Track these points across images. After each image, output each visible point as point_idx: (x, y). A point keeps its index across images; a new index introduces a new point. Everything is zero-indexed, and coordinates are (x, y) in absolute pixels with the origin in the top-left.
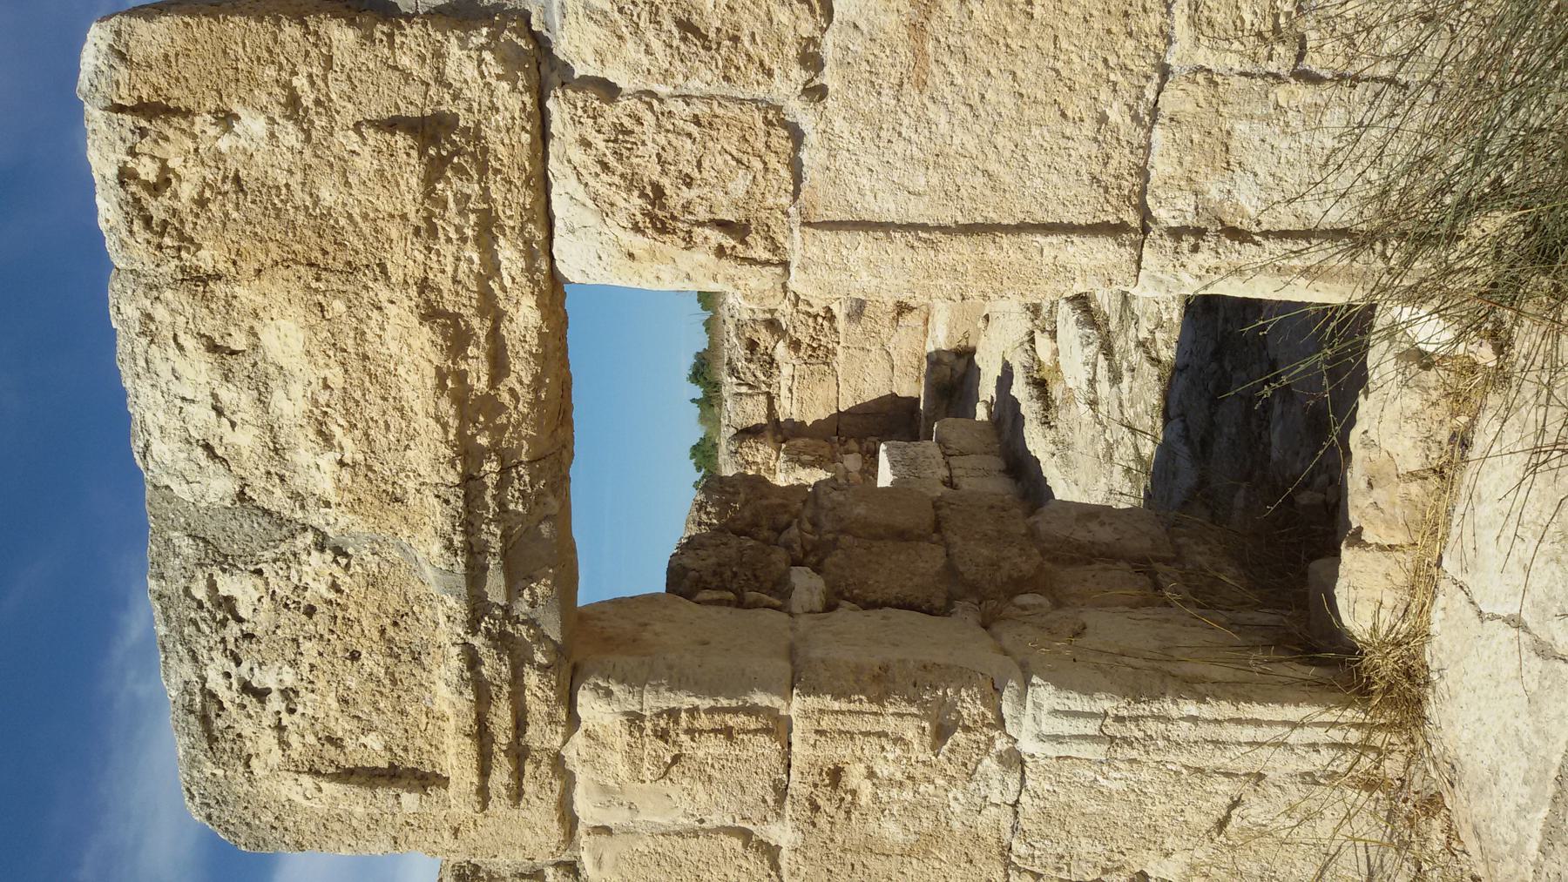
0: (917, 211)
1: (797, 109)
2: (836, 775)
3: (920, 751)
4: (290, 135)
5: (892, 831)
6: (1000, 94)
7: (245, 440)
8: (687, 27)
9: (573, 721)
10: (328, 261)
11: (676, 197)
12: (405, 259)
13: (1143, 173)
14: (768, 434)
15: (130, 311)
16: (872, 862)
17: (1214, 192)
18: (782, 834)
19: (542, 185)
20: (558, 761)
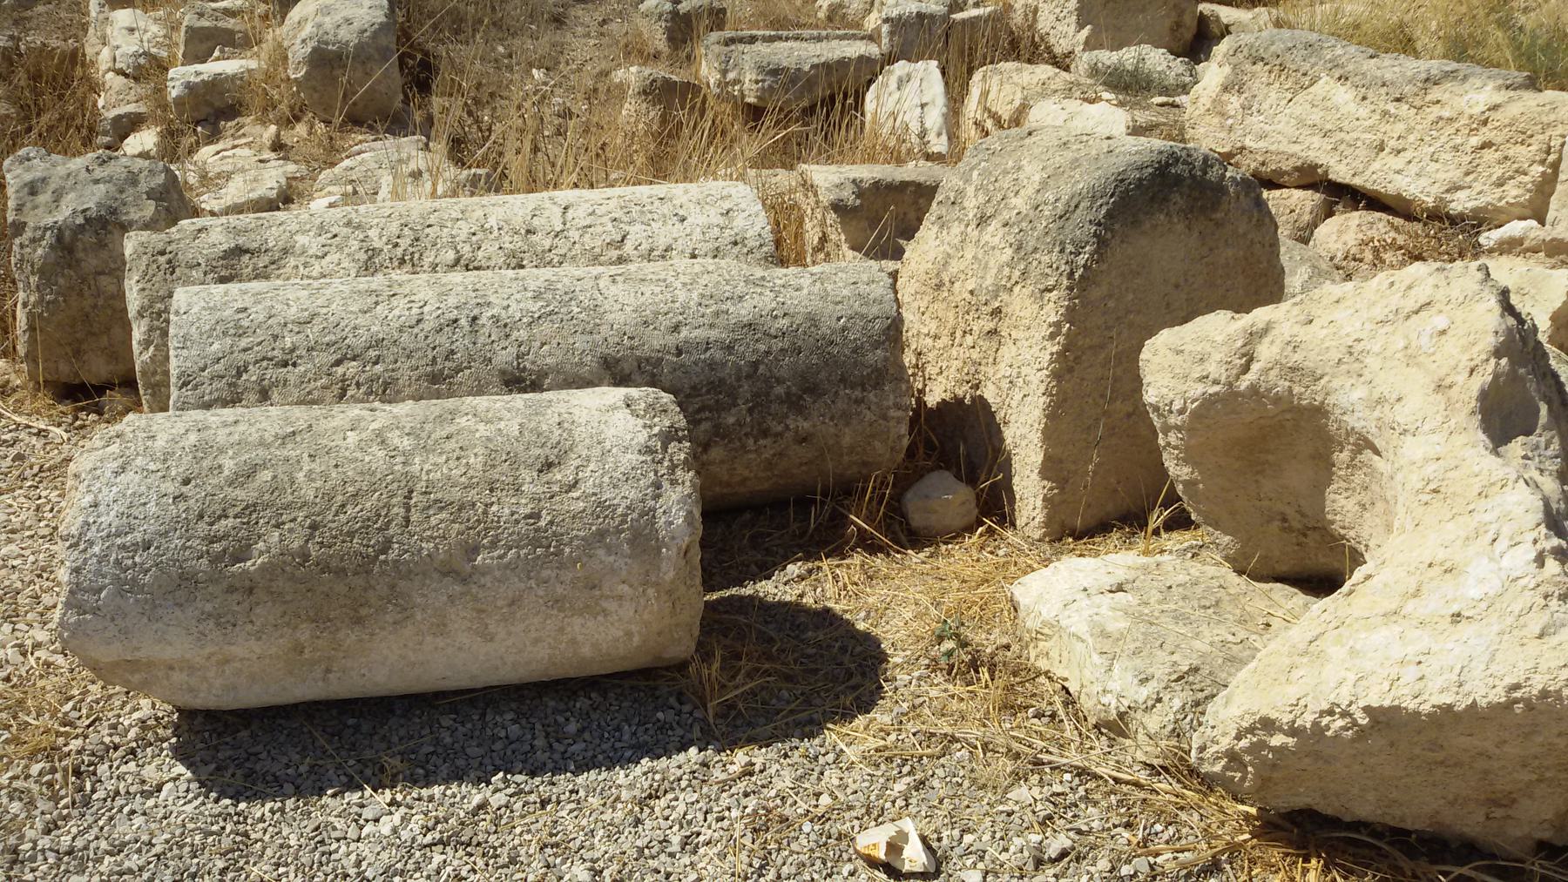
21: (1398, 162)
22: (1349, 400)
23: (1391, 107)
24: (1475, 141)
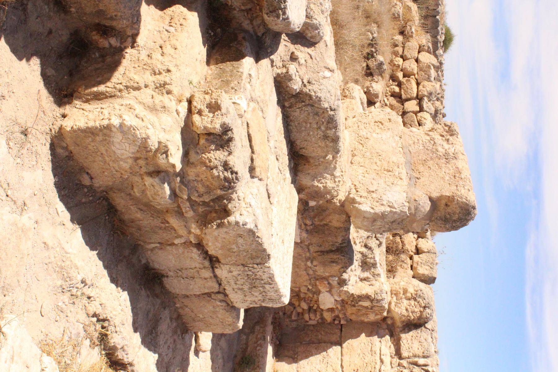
14: (399, 324)
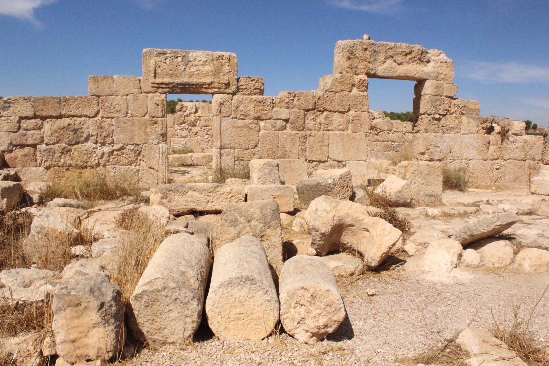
0: (222, 128)
1: (231, 117)
2: (155, 123)
3: (160, 132)
4: (227, 71)
5: (148, 130)
6: (233, 135)
7: (197, 63)
8: (238, 107)
9: (162, 93)
10: (216, 73)
11: (223, 106)
12: (216, 80)
13: (226, 148)
15: (210, 53)
16: (143, 128)
17: (225, 155)
18: (147, 117)
19: (223, 93)
20: (156, 92)
21: (214, 204)
22: (349, 221)
23: (209, 194)
24: (229, 196)
